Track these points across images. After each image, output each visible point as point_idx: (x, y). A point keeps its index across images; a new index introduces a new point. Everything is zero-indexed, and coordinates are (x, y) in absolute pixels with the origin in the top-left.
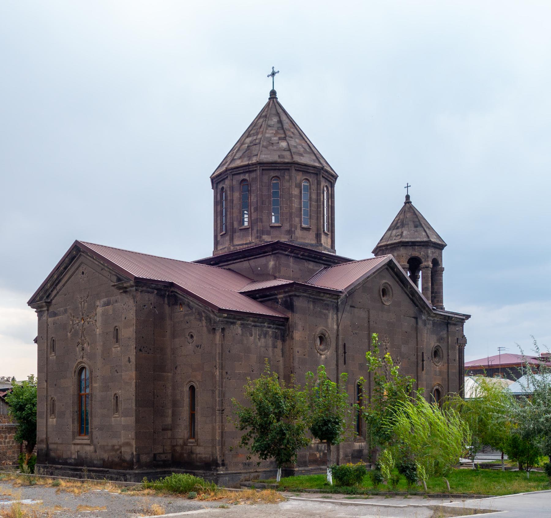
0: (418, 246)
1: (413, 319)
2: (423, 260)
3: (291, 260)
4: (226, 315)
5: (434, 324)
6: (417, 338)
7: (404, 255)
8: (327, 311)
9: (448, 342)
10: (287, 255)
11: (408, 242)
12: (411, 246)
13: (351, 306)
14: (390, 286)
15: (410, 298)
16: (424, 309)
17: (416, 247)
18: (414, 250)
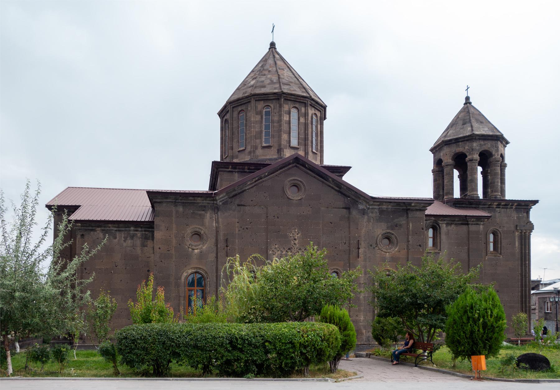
0: (462, 141)
1: (345, 210)
2: (467, 154)
3: (236, 174)
4: (80, 225)
5: (381, 212)
6: (349, 228)
7: (448, 153)
8: (203, 212)
9: (408, 229)
10: (229, 171)
11: (450, 140)
12: (454, 143)
13: (238, 205)
14: (301, 182)
15: (336, 190)
16: (360, 198)
17: (460, 143)
18: (458, 146)
